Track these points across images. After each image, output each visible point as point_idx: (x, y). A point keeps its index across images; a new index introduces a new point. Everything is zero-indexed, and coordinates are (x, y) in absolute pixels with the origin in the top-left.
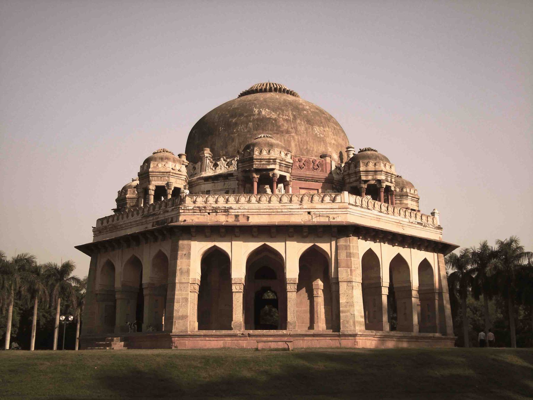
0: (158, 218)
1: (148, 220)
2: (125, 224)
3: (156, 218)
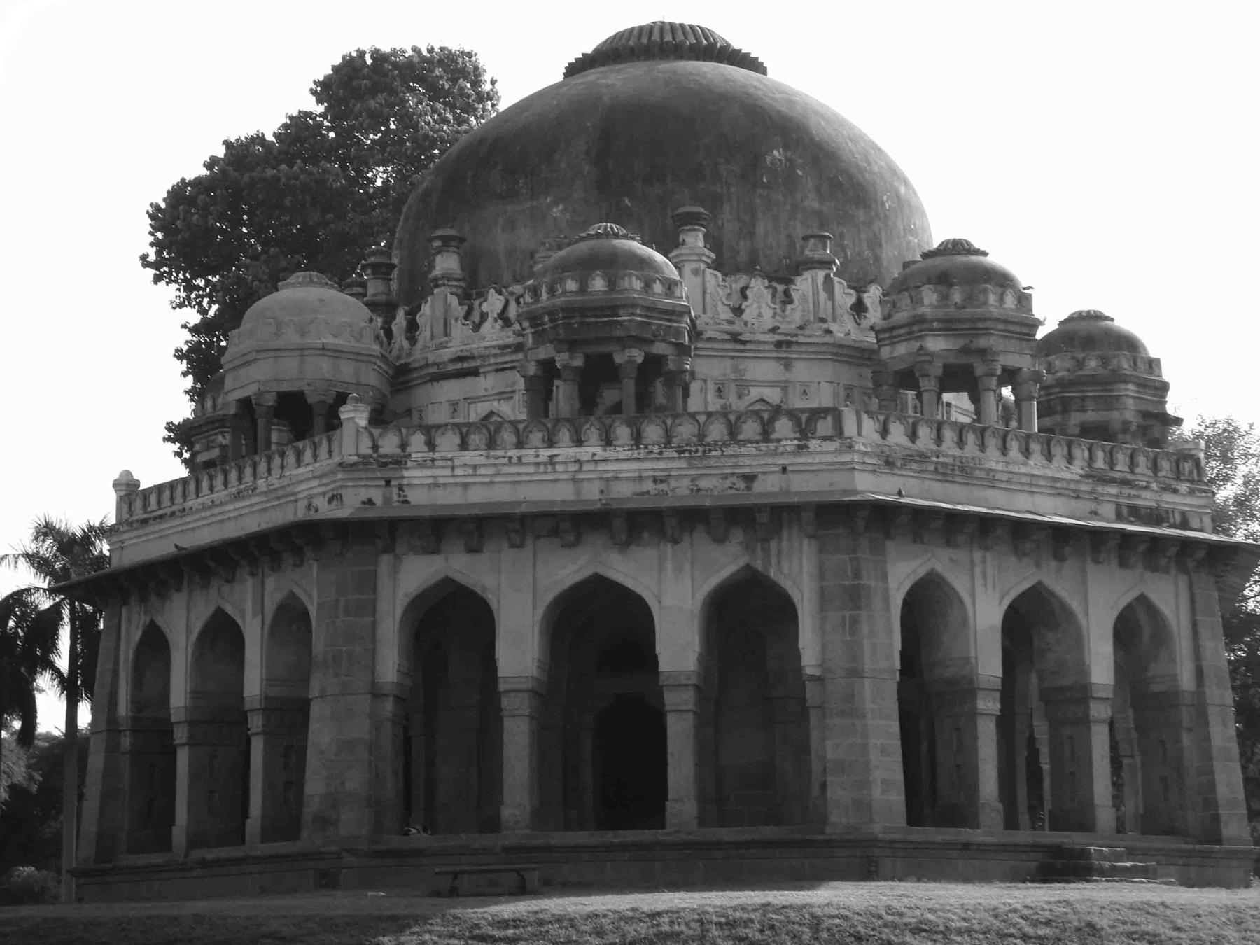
0: (1138, 497)
1: (1100, 489)
2: (1011, 473)
3: (1129, 495)
